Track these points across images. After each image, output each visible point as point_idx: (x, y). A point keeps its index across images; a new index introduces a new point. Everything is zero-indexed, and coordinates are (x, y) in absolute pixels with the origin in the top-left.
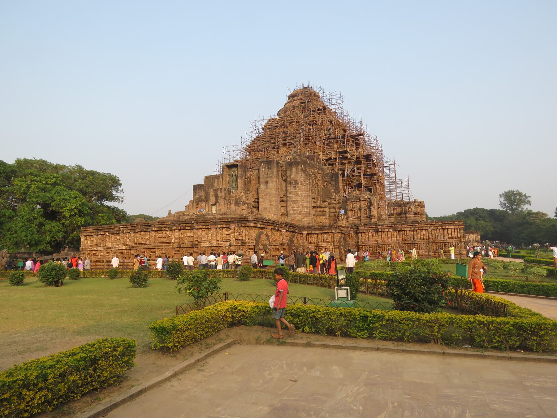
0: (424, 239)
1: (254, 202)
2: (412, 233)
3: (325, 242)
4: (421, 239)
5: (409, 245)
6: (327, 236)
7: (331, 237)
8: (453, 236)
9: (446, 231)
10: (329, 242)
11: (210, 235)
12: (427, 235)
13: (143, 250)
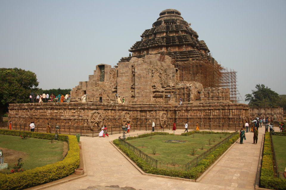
0: (217, 115)
1: (114, 88)
2: (209, 111)
3: (151, 116)
4: (215, 115)
5: (207, 119)
6: (152, 112)
7: (154, 112)
8: (236, 114)
9: (231, 110)
10: (153, 116)
11: (65, 112)
12: (219, 113)
13: (34, 119)
